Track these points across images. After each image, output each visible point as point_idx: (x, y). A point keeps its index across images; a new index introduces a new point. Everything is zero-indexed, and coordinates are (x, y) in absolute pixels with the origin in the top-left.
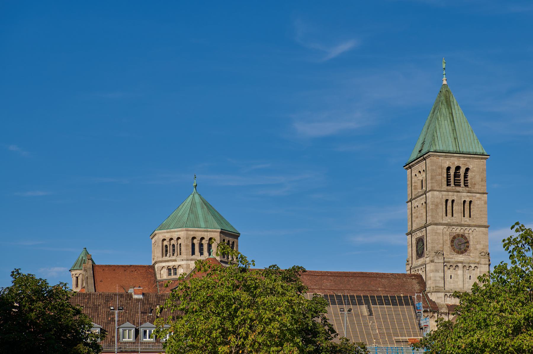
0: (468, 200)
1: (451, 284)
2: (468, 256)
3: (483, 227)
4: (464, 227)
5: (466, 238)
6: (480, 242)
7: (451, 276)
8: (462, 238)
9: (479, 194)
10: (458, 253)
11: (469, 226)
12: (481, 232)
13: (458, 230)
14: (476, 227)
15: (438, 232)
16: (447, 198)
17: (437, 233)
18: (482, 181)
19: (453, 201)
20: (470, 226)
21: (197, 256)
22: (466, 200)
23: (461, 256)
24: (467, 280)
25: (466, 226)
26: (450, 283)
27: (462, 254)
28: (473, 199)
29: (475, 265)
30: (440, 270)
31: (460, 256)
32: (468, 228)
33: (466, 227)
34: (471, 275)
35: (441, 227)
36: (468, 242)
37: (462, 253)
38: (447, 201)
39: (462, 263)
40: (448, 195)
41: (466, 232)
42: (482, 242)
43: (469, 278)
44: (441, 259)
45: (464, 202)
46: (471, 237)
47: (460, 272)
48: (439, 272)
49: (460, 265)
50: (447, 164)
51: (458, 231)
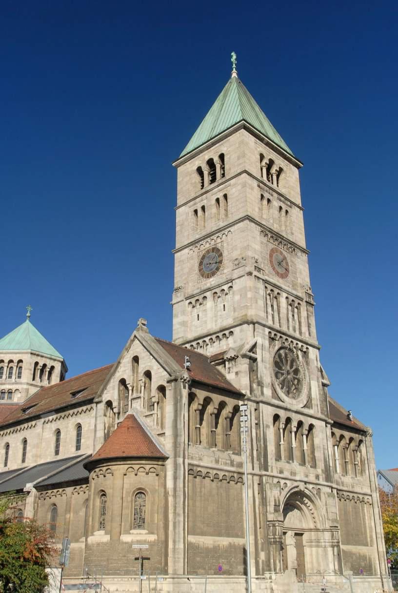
3: (240, 222)
5: (218, 250)
7: (198, 316)
10: (208, 277)
13: (206, 245)
15: (182, 259)
17: (180, 261)
19: (203, 208)
21: (38, 381)
22: (219, 197)
26: (196, 327)
27: (213, 276)
30: (180, 313)
32: (220, 234)
35: (186, 251)
36: (221, 255)
37: (213, 274)
39: (209, 290)
41: (218, 242)
42: (238, 245)
44: (180, 296)
47: (209, 303)
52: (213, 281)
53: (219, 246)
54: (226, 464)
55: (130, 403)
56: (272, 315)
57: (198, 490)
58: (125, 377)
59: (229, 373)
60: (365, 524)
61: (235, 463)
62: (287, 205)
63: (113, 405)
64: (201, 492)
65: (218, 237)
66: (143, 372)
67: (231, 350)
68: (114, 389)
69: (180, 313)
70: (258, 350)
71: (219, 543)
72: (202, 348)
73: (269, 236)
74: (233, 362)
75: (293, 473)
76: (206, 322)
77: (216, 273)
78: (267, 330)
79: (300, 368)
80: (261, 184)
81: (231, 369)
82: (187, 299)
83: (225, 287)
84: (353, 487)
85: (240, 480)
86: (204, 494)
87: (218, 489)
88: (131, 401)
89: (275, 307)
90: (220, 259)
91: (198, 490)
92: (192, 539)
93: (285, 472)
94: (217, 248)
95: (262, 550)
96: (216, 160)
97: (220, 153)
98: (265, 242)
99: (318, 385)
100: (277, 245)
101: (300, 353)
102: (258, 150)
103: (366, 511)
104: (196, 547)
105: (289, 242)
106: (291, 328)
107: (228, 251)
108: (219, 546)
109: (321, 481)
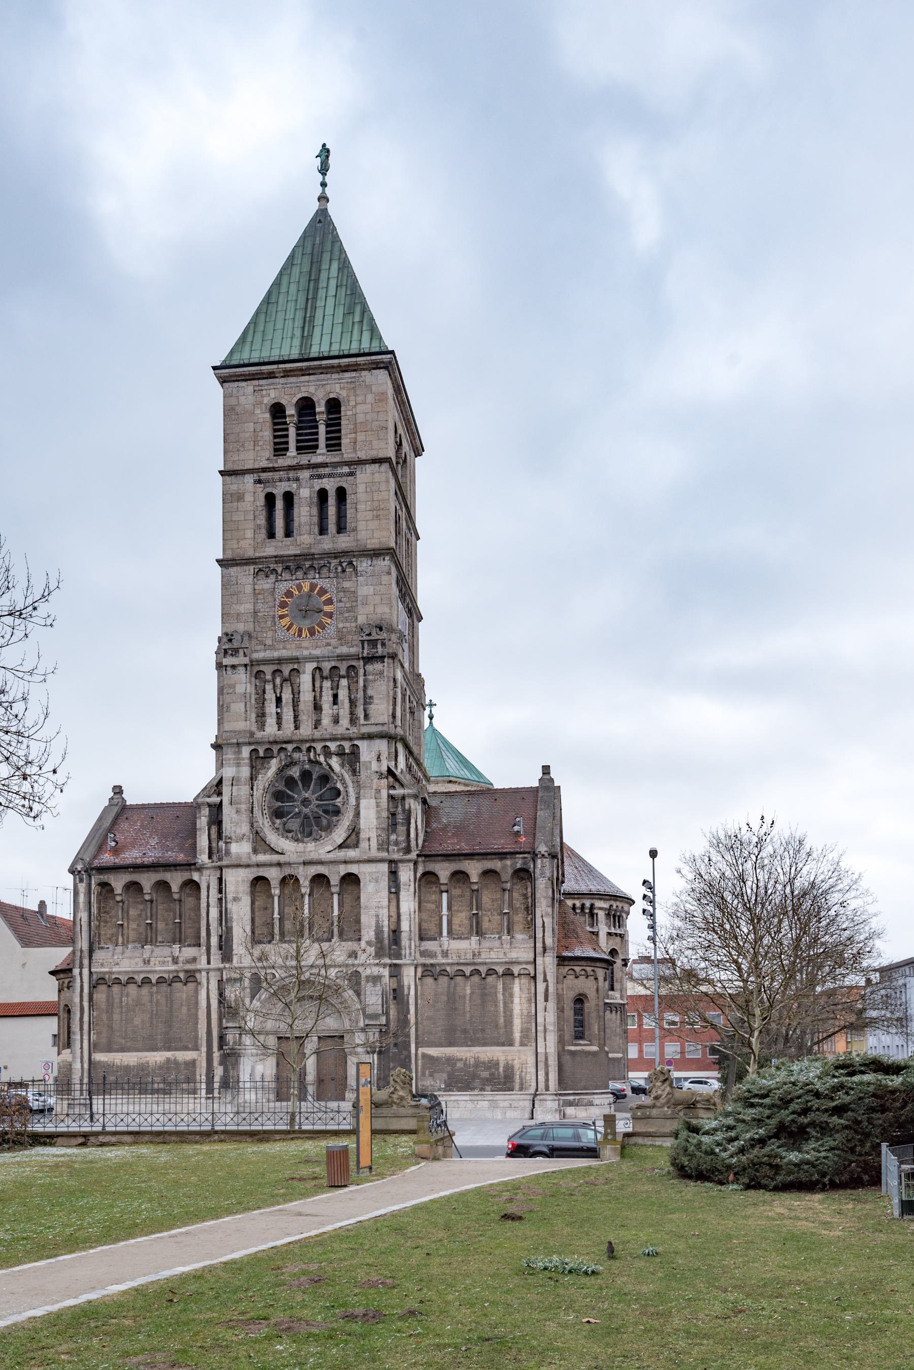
56: (277, 713)
57: (117, 1000)
70: (226, 789)
71: (147, 1059)
85: (192, 979)
86: (127, 1004)
89: (287, 696)
91: (117, 1000)
92: (99, 1057)
95: (221, 1064)
104: (109, 1065)
108: (148, 1063)
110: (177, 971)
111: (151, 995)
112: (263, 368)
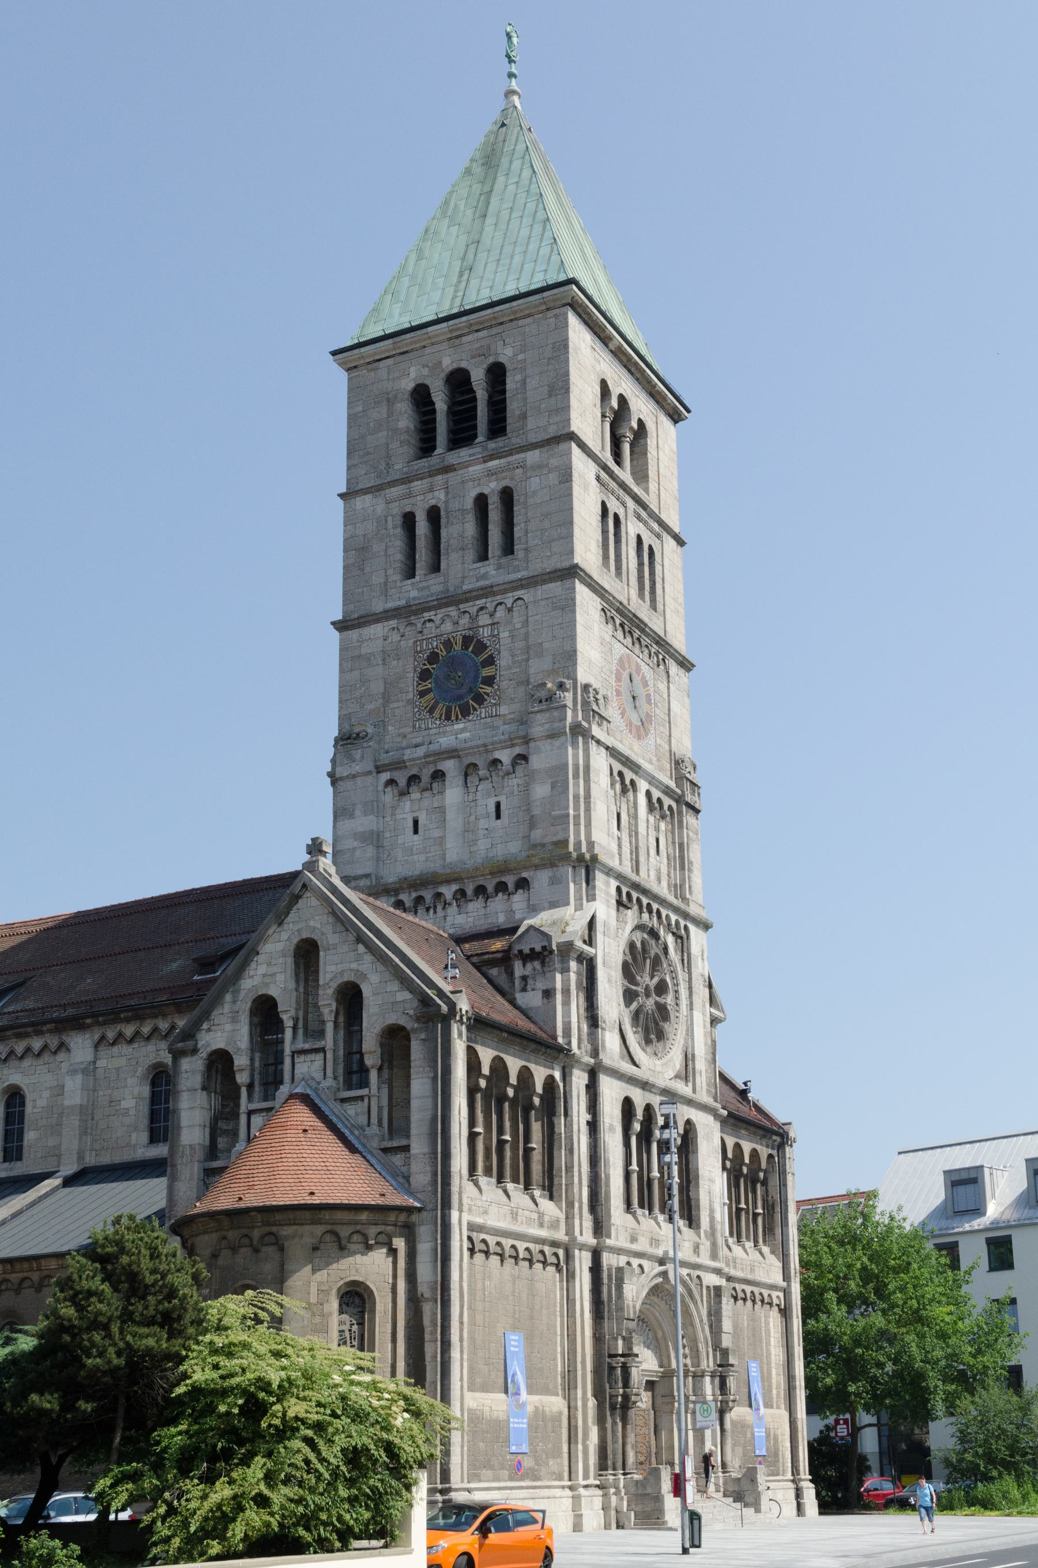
0: (492, 488)
1: (416, 857)
2: (489, 720)
4: (471, 603)
5: (481, 647)
6: (541, 644)
7: (416, 823)
8: (467, 648)
9: (537, 452)
10: (448, 718)
11: (488, 591)
12: (544, 603)
14: (522, 587)
15: (363, 651)
16: (408, 509)
17: (360, 656)
18: (550, 395)
20: (494, 594)
22: (486, 491)
23: (461, 726)
24: (483, 823)
25: (478, 598)
26: (410, 851)
27: (464, 716)
28: (512, 479)
29: (517, 750)
30: (359, 806)
31: (456, 727)
32: (490, 603)
33: (477, 602)
34: (503, 799)
36: (490, 661)
37: (466, 712)
38: (409, 520)
39: (452, 753)
40: (410, 495)
41: (481, 623)
42: (546, 645)
43: (494, 815)
44: (362, 757)
45: (481, 502)
46: (502, 635)
47: (453, 794)
48: (352, 816)
49: (449, 766)
50: (413, 375)
51: (448, 627)
52: (463, 730)
53: (485, 633)
54: (529, 1221)
55: (287, 1061)
58: (274, 992)
59: (524, 990)
60: (769, 1354)
61: (546, 1218)
62: (652, 530)
63: (236, 1063)
64: (484, 1289)
65: (482, 609)
66: (334, 985)
67: (532, 932)
68: (234, 1020)
69: (359, 806)
72: (432, 911)
73: (618, 622)
74: (537, 964)
75: (655, 1242)
76: (441, 840)
77: (475, 709)
78: (614, 884)
79: (668, 979)
80: (603, 475)
81: (530, 982)
82: (379, 769)
83: (505, 756)
84: (752, 1270)
87: (514, 1284)
88: (293, 1057)
90: (486, 672)
93: (641, 1239)
94: (479, 641)
96: (478, 376)
97: (491, 360)
98: (608, 638)
99: (704, 1021)
100: (630, 645)
101: (670, 940)
102: (598, 369)
103: (771, 1325)
105: (654, 638)
106: (653, 873)
107: (513, 656)
109: (704, 1259)
110: (542, 1241)
111: (515, 1279)
112: (608, 326)
